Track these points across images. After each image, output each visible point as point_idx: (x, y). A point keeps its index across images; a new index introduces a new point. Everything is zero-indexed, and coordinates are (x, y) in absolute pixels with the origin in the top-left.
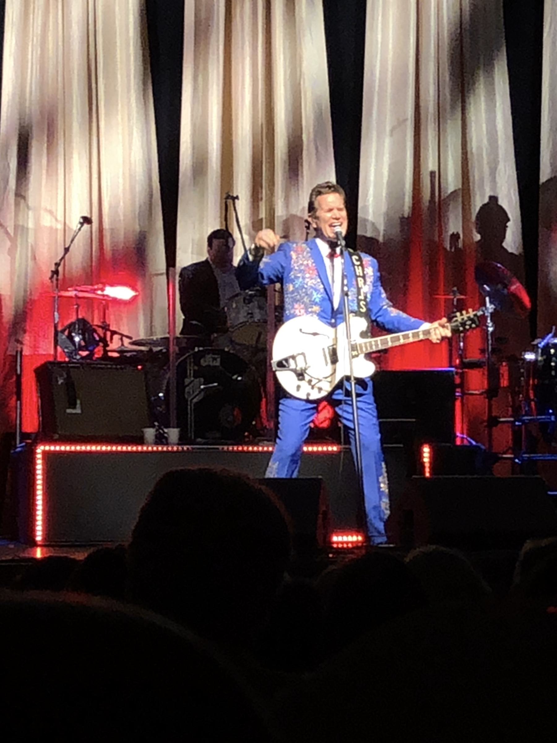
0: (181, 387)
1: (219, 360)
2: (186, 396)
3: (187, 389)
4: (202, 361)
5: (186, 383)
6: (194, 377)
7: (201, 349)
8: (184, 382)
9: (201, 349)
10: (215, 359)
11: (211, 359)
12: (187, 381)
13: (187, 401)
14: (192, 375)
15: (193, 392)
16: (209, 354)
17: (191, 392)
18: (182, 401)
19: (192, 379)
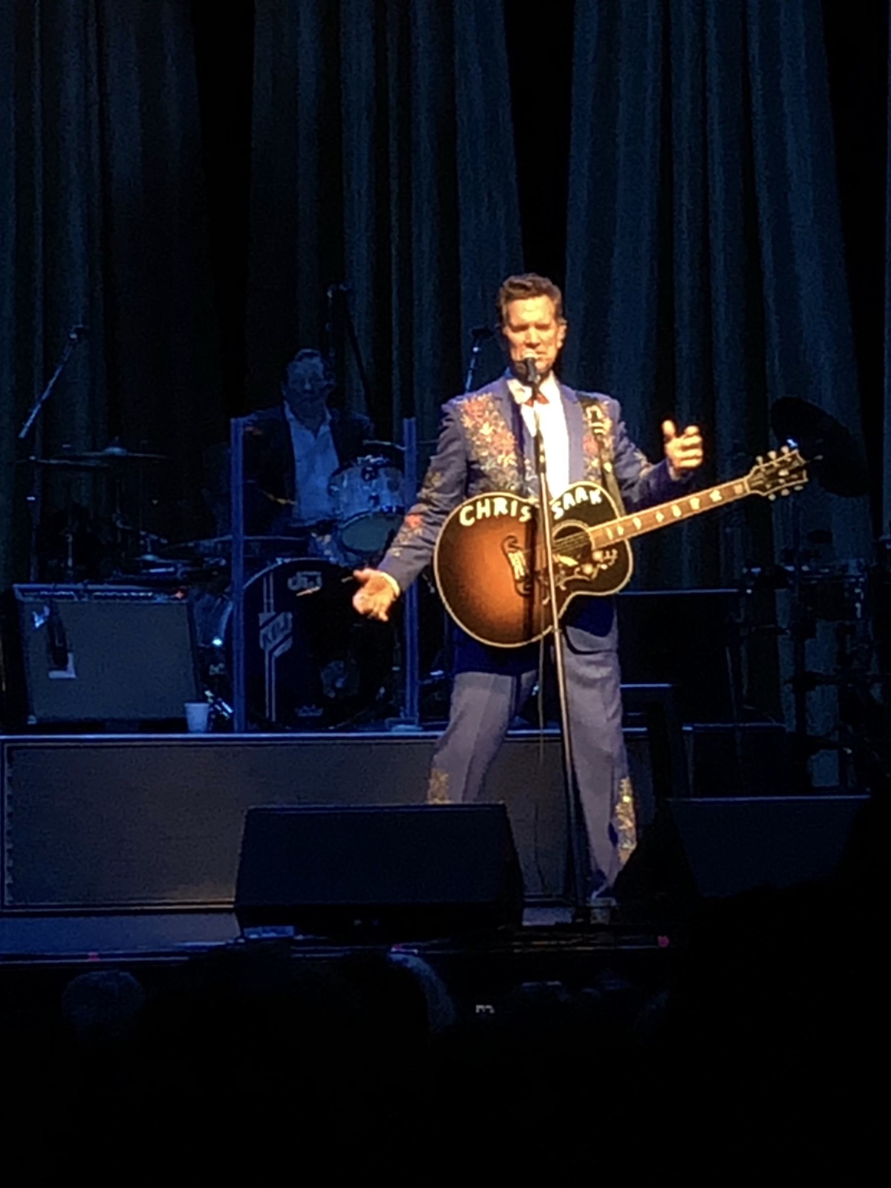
0: (252, 629)
1: (319, 580)
2: (262, 645)
3: (262, 632)
4: (290, 581)
5: (261, 624)
6: (275, 610)
7: (287, 560)
8: (257, 619)
9: (287, 560)
10: (312, 579)
11: (305, 579)
12: (263, 617)
13: (262, 652)
14: (272, 606)
15: (274, 637)
16: (302, 570)
17: (270, 636)
18: (254, 655)
19: (273, 613)
